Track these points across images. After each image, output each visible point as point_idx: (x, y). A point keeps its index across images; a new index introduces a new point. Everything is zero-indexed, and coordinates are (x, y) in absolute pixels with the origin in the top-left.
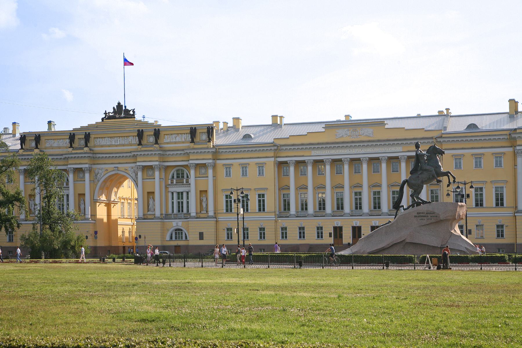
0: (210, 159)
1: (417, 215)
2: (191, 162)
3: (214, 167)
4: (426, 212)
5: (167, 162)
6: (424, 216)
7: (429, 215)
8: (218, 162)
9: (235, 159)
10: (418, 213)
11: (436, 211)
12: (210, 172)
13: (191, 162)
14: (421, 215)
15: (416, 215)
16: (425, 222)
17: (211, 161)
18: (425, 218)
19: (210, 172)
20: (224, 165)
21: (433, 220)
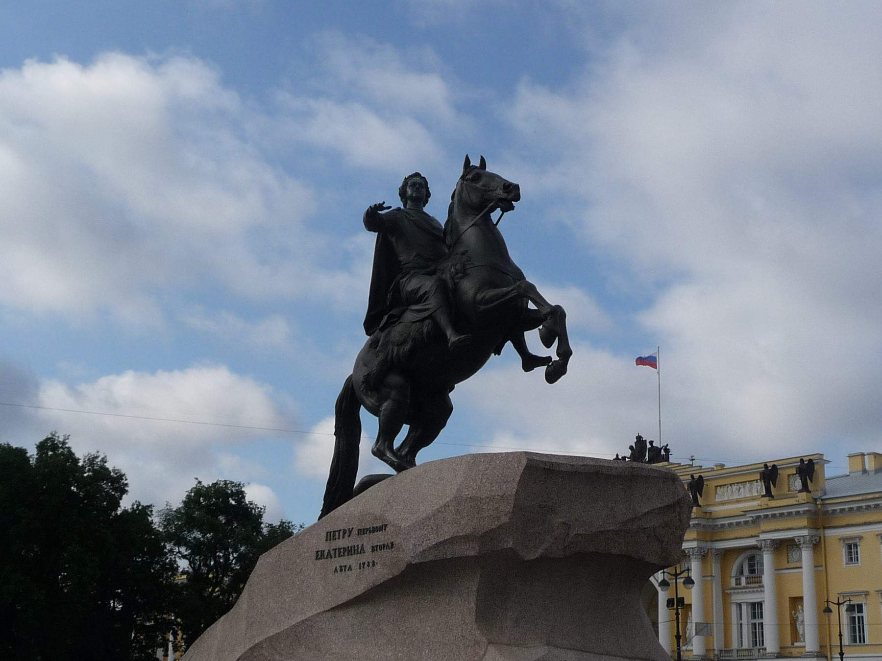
0: (805, 528)
2: (763, 537)
3: (817, 545)
4: (356, 526)
5: (721, 540)
6: (349, 551)
7: (368, 541)
8: (829, 533)
9: (866, 524)
12: (806, 555)
13: (763, 537)
14: (342, 543)
15: (324, 546)
16: (355, 584)
17: (805, 532)
18: (351, 561)
19: (806, 555)
20: (843, 539)
21: (380, 573)
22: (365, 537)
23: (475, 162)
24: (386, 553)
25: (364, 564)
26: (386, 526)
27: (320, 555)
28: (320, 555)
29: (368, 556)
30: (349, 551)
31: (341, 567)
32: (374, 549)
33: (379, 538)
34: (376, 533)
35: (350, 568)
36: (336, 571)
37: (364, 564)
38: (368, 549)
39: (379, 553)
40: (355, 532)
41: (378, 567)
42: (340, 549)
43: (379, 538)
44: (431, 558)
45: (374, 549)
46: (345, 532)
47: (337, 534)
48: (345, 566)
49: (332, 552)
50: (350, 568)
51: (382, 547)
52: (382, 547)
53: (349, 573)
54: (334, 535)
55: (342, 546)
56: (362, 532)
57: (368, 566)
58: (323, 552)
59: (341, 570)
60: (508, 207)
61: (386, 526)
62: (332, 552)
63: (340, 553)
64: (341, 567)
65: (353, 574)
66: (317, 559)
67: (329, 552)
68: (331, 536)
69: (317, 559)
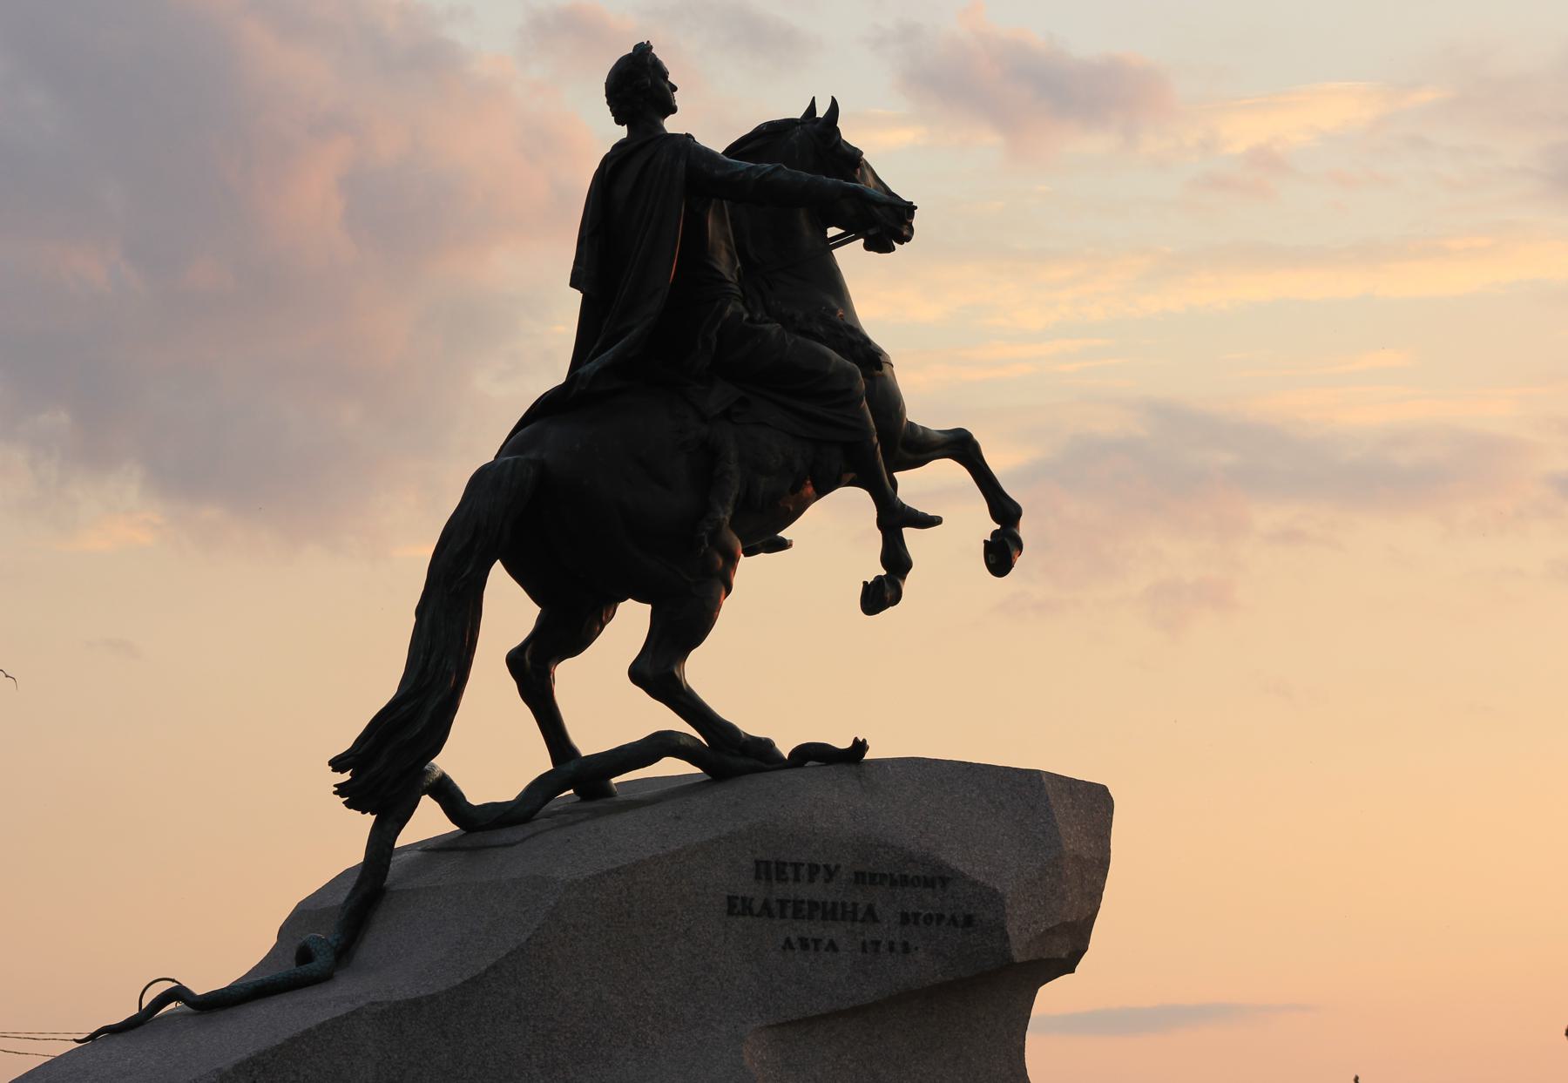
6: (830, 912)
10: (767, 870)
11: (953, 857)
18: (835, 931)
23: (821, 112)
25: (877, 943)
26: (944, 881)
27: (737, 906)
28: (737, 906)
30: (830, 912)
32: (905, 919)
35: (832, 946)
37: (877, 943)
42: (797, 904)
44: (1032, 956)
45: (905, 919)
46: (814, 869)
47: (789, 870)
48: (817, 942)
49: (775, 906)
50: (832, 946)
56: (859, 878)
57: (891, 949)
60: (881, 244)
61: (944, 881)
62: (775, 906)
69: (730, 913)
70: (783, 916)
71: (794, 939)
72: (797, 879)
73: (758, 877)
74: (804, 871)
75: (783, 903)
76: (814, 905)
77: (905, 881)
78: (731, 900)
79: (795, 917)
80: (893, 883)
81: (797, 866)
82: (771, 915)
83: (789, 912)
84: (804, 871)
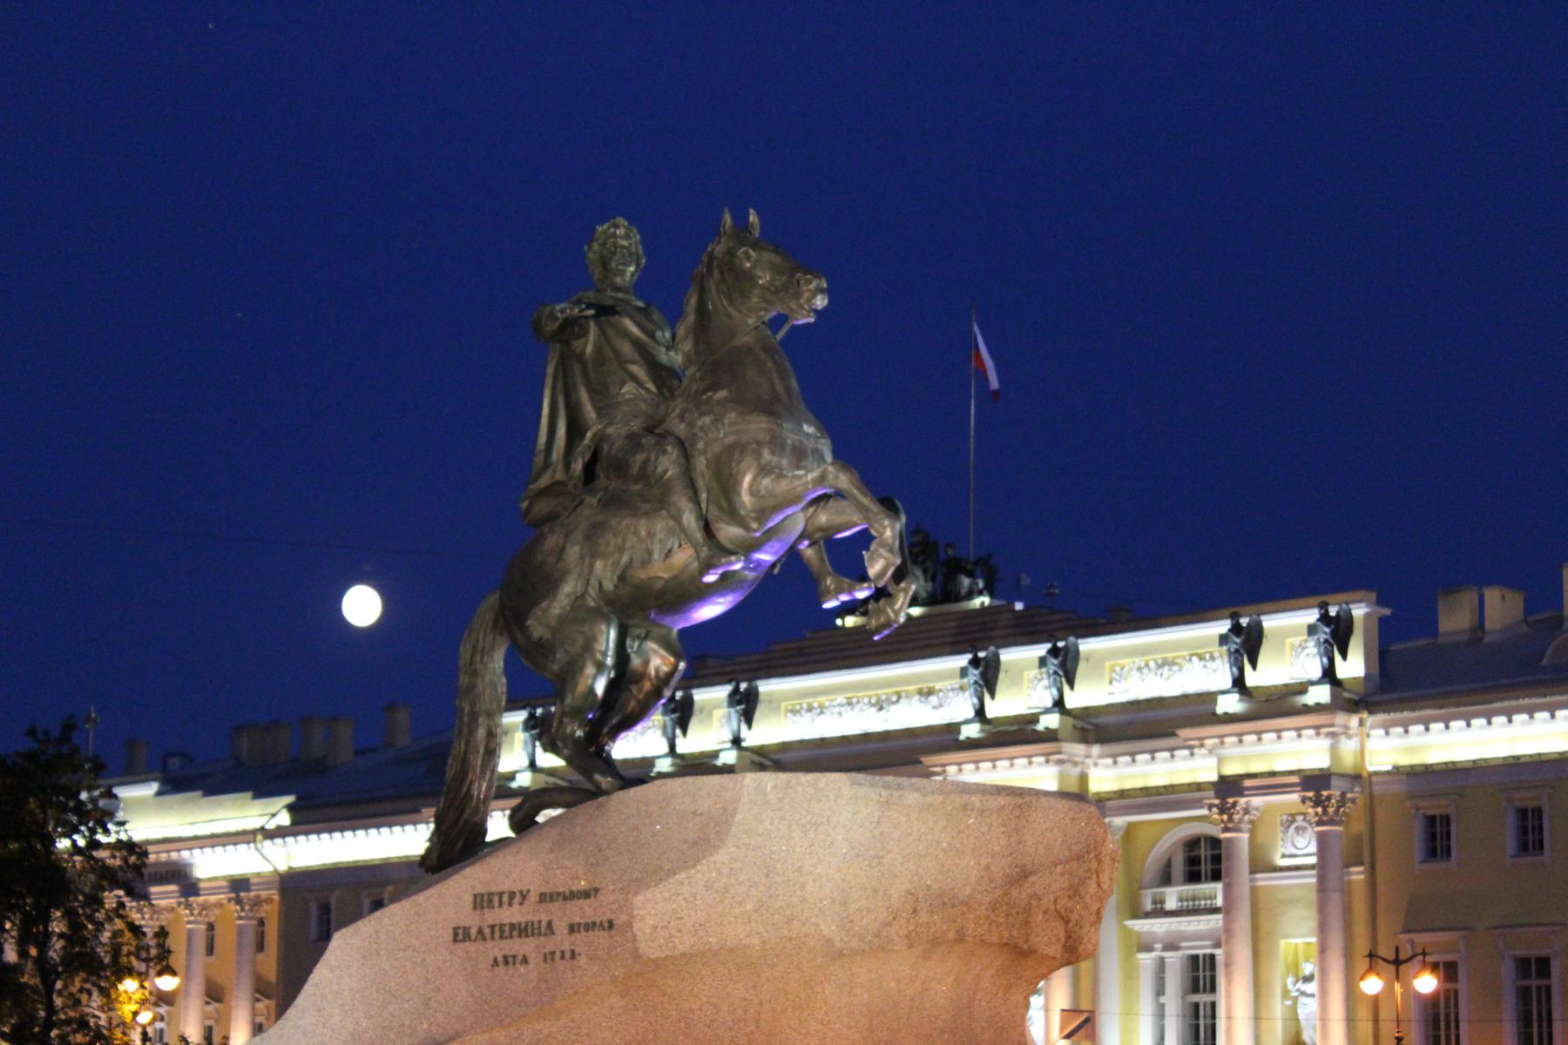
1: (472, 920)
7: (562, 914)
22: (555, 906)
24: (600, 937)
25: (553, 953)
28: (460, 935)
29: (562, 940)
31: (505, 958)
32: (572, 929)
33: (584, 911)
34: (575, 902)
36: (496, 962)
37: (553, 953)
38: (561, 927)
39: (581, 936)
40: (533, 898)
41: (583, 961)
42: (502, 926)
43: (584, 911)
45: (572, 929)
46: (512, 895)
47: (496, 899)
48: (514, 957)
49: (487, 931)
51: (591, 926)
52: (591, 926)
53: (522, 969)
54: (490, 901)
55: (506, 921)
56: (544, 898)
57: (563, 957)
58: (466, 930)
59: (506, 963)
62: (487, 931)
63: (502, 931)
64: (505, 958)
65: (532, 971)
66: (455, 940)
67: (480, 931)
68: (482, 902)
70: (493, 939)
71: (500, 959)
72: (501, 905)
73: (475, 908)
74: (505, 898)
75: (492, 927)
76: (512, 926)
77: (573, 895)
78: (456, 930)
79: (501, 937)
80: (565, 898)
81: (501, 894)
82: (484, 939)
83: (497, 935)
84: (505, 898)
